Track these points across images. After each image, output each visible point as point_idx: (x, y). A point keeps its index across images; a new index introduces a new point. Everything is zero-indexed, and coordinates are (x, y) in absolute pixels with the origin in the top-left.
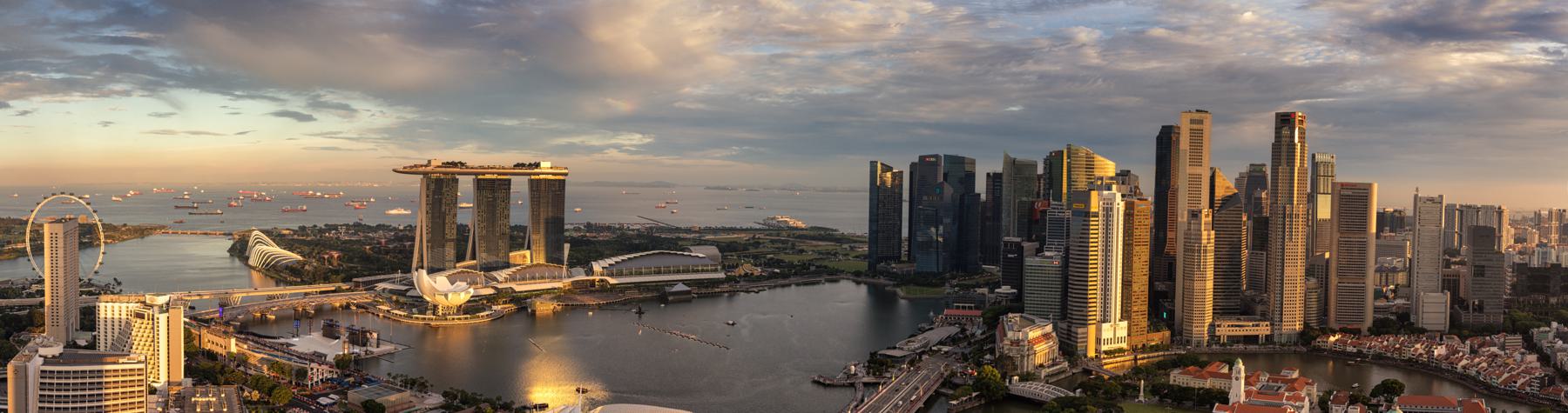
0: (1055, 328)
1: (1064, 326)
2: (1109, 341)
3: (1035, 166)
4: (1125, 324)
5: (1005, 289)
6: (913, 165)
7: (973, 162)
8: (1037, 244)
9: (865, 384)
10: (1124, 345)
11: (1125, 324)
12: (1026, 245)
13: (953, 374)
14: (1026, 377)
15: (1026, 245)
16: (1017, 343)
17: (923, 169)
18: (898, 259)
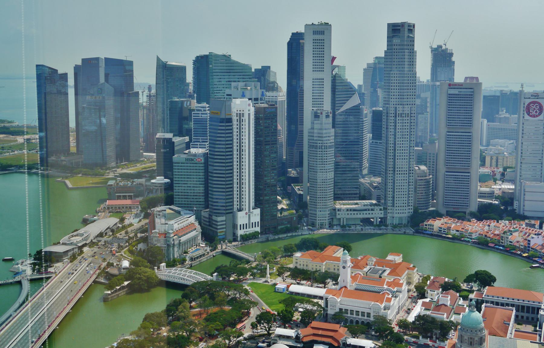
0: (198, 218)
1: (205, 213)
2: (243, 227)
3: (183, 69)
4: (258, 211)
5: (160, 180)
6: (77, 68)
7: (131, 63)
8: (187, 139)
9: (32, 281)
10: (258, 229)
11: (258, 211)
12: (177, 140)
13: (110, 265)
14: (171, 264)
15: (177, 140)
16: (166, 235)
17: (87, 68)
18: (67, 151)
